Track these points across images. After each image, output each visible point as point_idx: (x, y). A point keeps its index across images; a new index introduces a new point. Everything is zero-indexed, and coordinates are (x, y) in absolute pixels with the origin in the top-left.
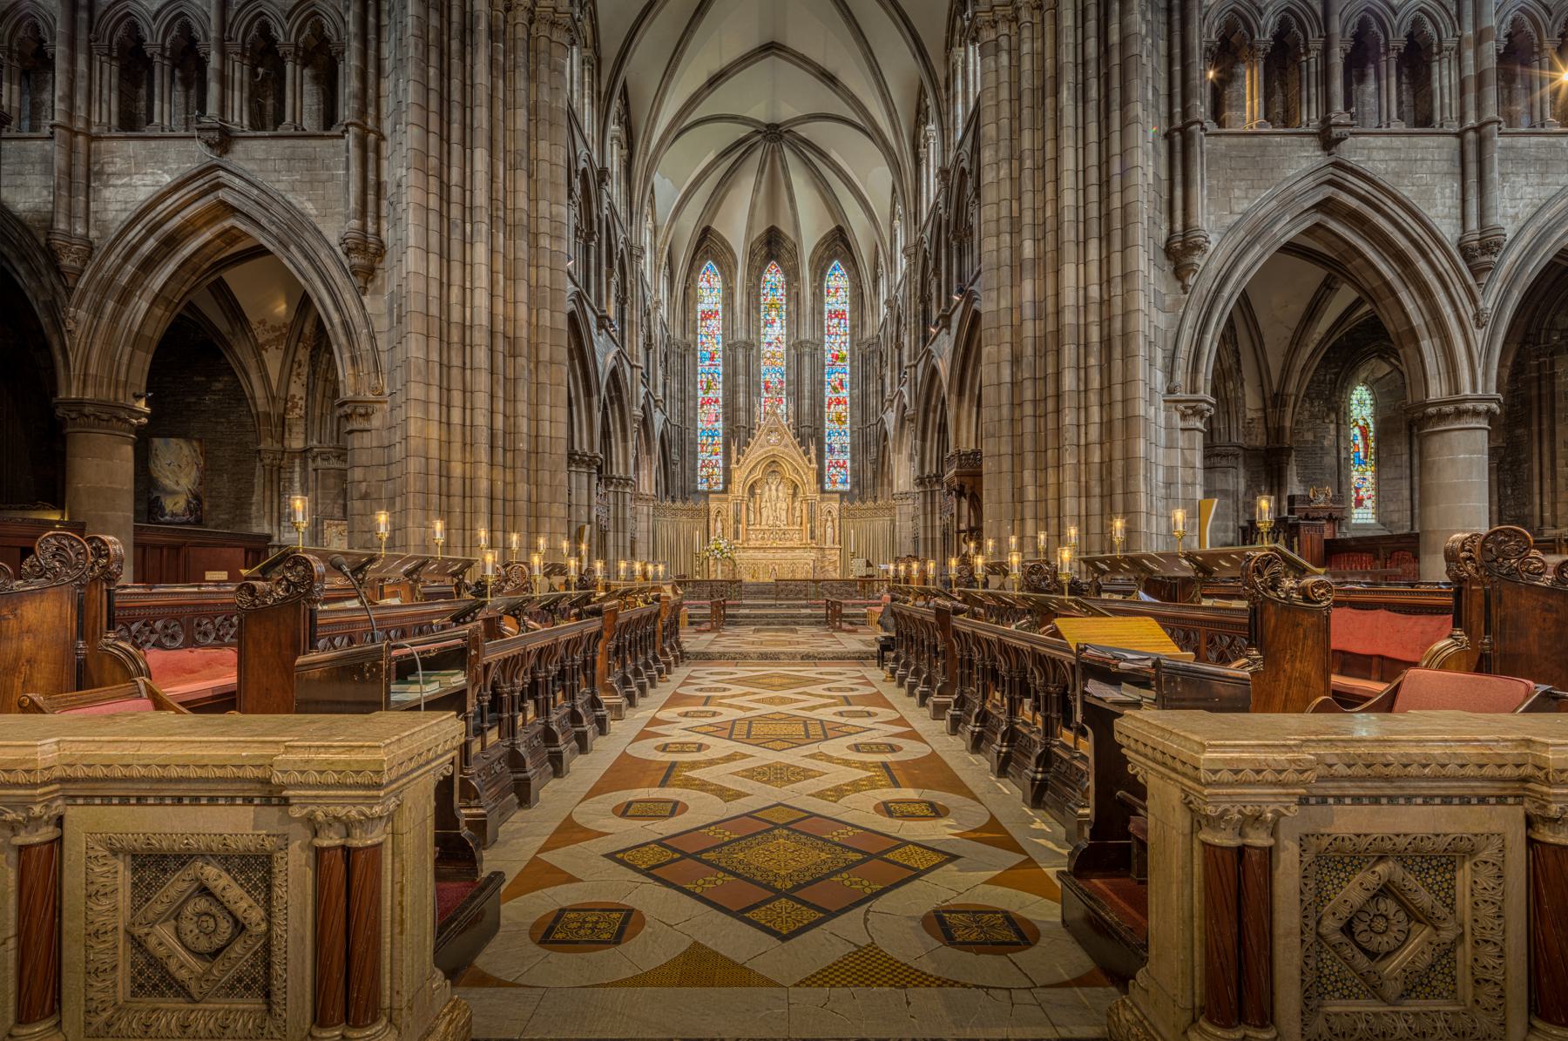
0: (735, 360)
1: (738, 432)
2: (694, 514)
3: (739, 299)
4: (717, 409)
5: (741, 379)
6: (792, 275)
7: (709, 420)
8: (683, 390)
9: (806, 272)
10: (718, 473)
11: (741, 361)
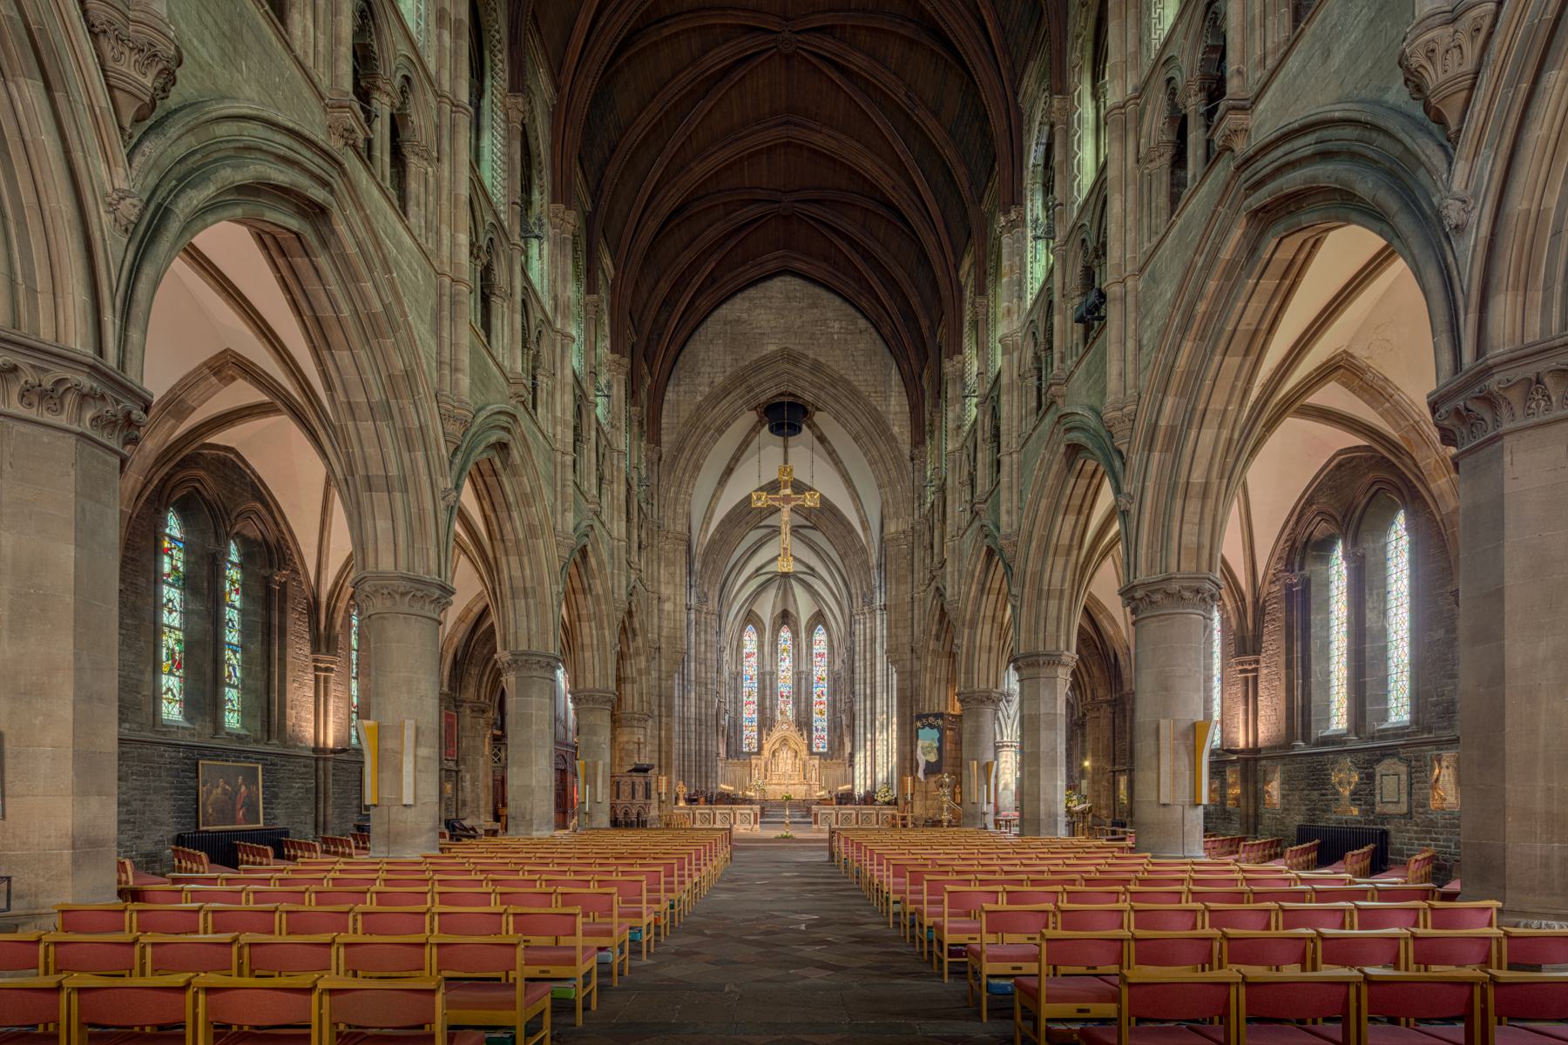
0: (764, 681)
1: (766, 723)
2: (744, 766)
3: (767, 649)
4: (754, 707)
5: (768, 692)
6: (796, 634)
7: (750, 713)
8: (736, 698)
9: (803, 635)
10: (755, 743)
11: (768, 682)
